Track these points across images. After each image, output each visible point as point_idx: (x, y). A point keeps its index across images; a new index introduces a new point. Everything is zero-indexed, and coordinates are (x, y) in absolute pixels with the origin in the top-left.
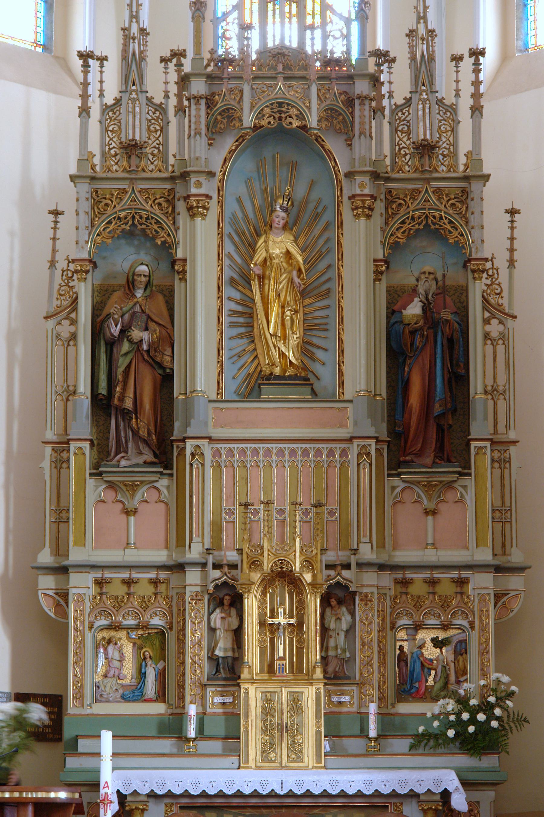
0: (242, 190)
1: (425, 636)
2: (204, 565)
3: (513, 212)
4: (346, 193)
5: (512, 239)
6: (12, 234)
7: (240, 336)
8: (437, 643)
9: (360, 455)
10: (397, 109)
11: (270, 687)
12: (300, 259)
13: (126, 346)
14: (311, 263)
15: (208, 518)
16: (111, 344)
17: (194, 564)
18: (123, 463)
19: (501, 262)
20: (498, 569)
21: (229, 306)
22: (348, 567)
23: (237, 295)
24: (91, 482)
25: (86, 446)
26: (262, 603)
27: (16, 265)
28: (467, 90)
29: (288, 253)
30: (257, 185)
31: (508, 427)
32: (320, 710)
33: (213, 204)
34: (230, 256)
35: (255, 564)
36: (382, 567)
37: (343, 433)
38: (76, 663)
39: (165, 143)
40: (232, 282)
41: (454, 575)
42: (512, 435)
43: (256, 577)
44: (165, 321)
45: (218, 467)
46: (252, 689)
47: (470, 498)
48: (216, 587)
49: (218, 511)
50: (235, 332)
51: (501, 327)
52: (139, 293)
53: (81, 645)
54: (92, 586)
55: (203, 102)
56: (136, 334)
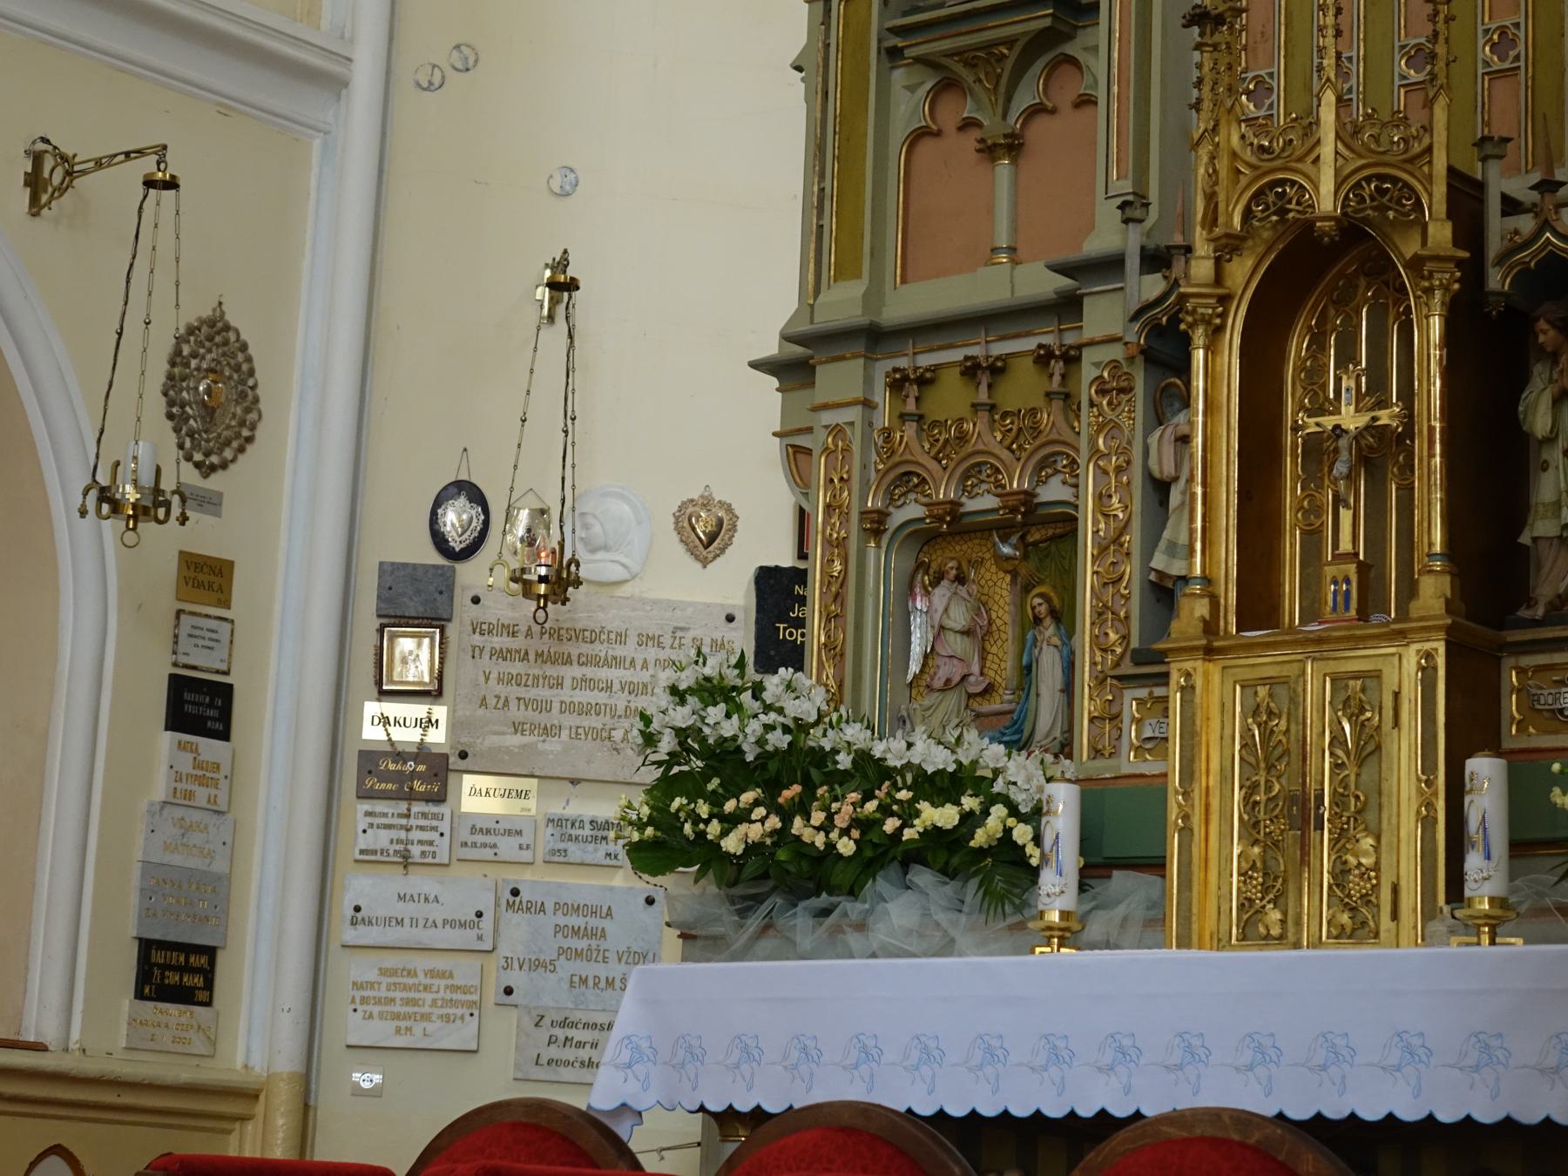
11: (1267, 664)
32: (1435, 736)
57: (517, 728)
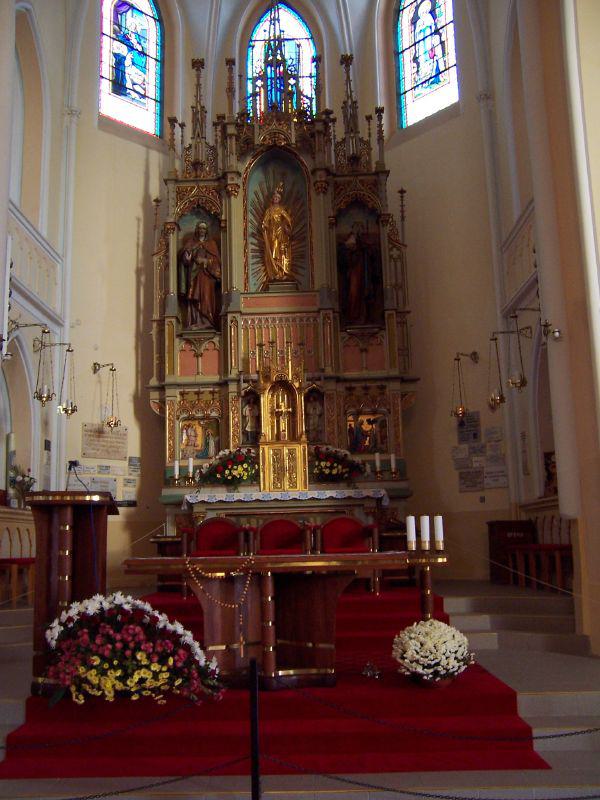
0: (257, 188)
1: (363, 418)
2: (238, 381)
3: (402, 192)
4: (312, 182)
5: (402, 206)
6: (139, 220)
7: (258, 263)
8: (369, 422)
9: (324, 318)
10: (337, 144)
12: (289, 220)
13: (195, 267)
14: (295, 223)
15: (242, 356)
16: (188, 266)
17: (232, 380)
18: (194, 328)
19: (397, 217)
20: (403, 380)
21: (250, 230)
22: (319, 379)
23: (255, 241)
24: (177, 341)
25: (174, 320)
26: (272, 401)
27: (141, 235)
28: (375, 136)
29: (282, 217)
30: (265, 185)
31: (404, 303)
33: (241, 190)
34: (251, 222)
35: (267, 378)
36: (338, 380)
37: (315, 308)
38: (170, 438)
39: (217, 164)
40: (253, 235)
41: (379, 384)
42: (407, 309)
43: (269, 386)
44: (217, 253)
45: (246, 329)
46: (266, 448)
47: (385, 342)
48: (246, 392)
49: (247, 354)
50: (255, 260)
51: (398, 252)
52: (202, 240)
53: (173, 429)
54: (178, 396)
55: (234, 138)
56: (200, 260)
57: (93, 449)
